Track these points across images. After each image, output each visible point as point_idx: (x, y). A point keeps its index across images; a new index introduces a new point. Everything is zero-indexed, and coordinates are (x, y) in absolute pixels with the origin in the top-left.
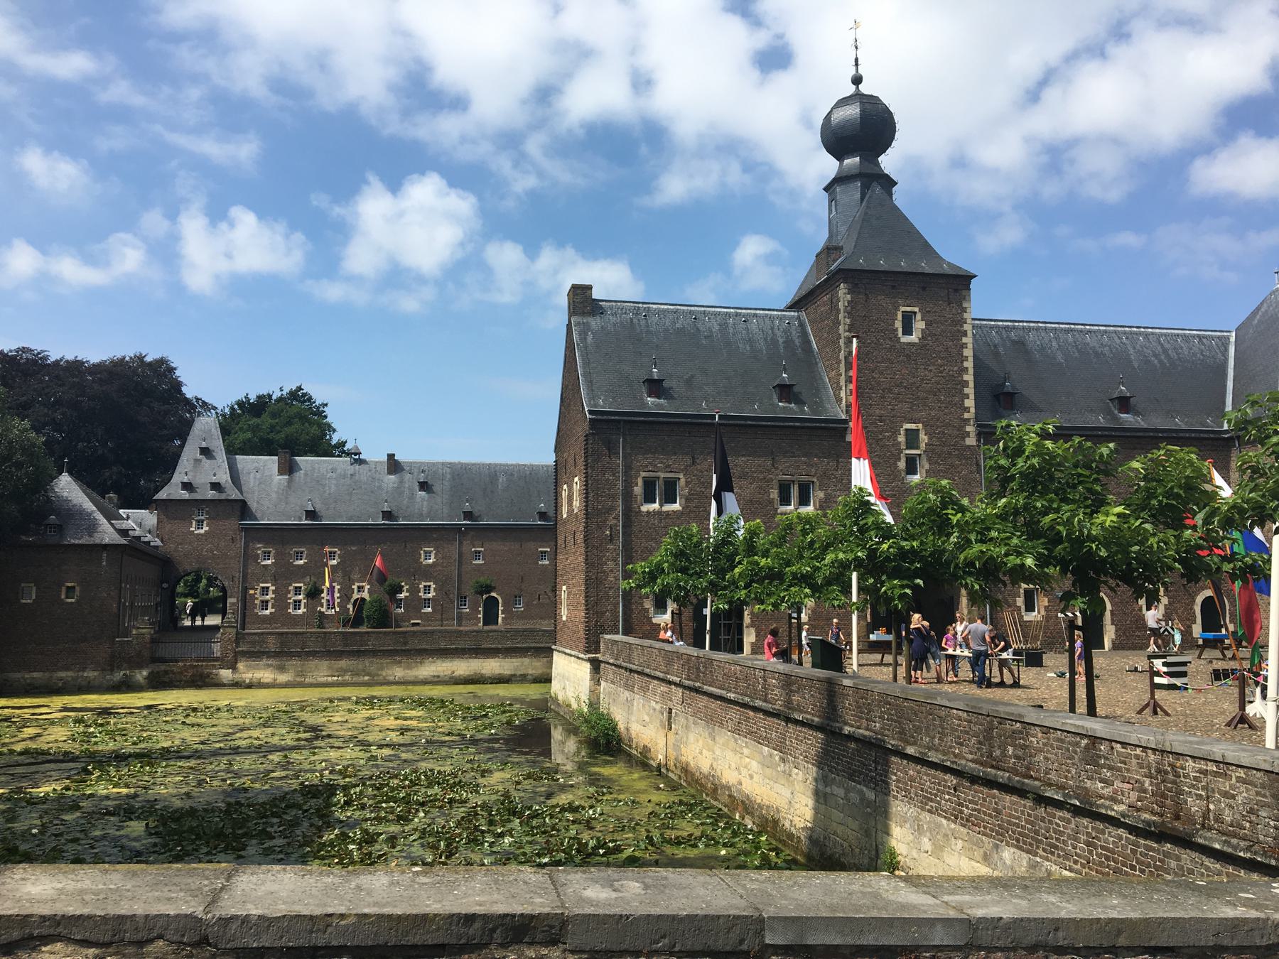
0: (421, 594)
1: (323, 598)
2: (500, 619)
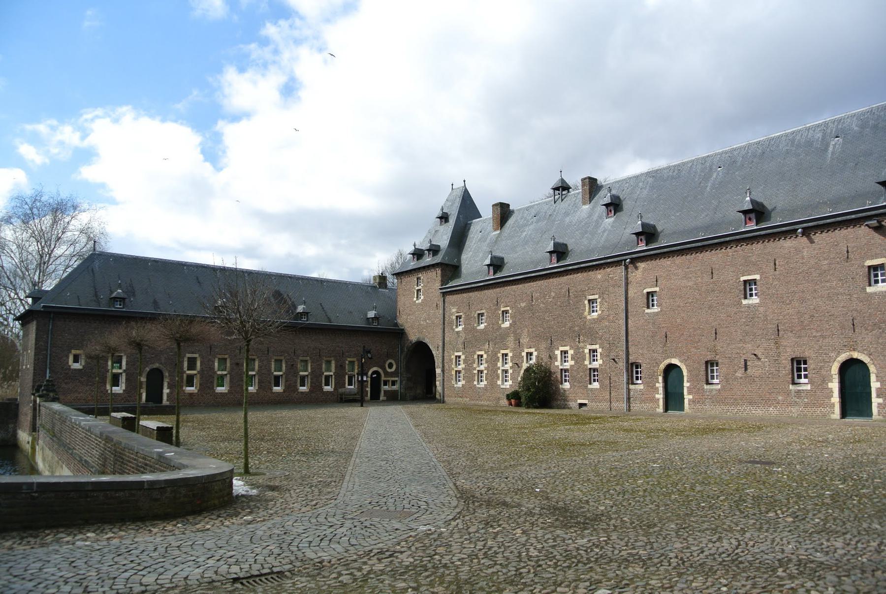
0: (587, 362)
1: (499, 368)
2: (686, 402)
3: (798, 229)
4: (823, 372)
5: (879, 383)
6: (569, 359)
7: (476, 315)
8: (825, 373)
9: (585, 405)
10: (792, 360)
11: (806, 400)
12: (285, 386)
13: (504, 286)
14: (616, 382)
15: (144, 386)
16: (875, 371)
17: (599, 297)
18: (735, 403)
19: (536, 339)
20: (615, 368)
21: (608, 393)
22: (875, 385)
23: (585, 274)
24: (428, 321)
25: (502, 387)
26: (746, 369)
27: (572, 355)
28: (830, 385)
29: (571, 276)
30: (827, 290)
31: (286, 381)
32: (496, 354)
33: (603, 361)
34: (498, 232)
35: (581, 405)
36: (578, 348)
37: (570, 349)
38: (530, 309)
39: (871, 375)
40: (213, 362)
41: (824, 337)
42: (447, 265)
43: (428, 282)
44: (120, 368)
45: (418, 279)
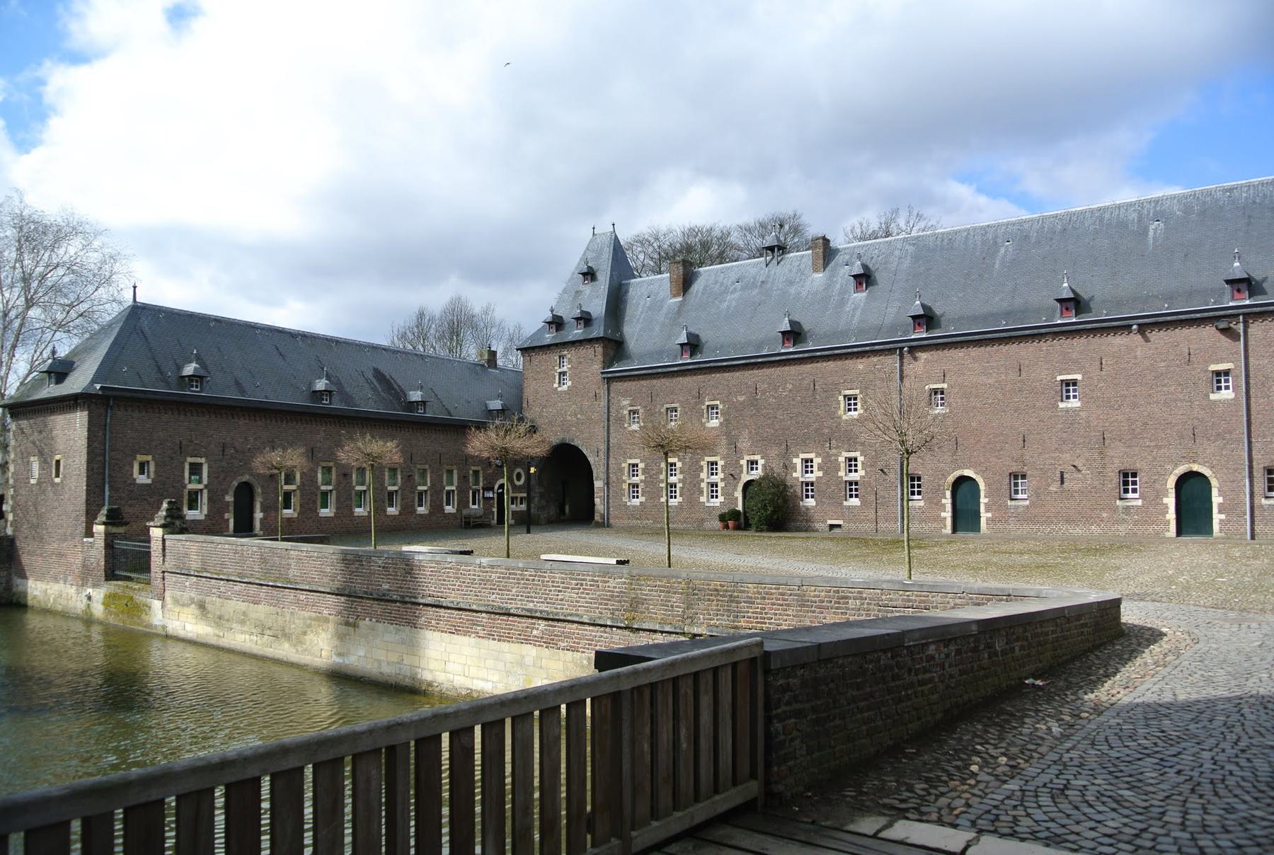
0: (842, 473)
1: (703, 480)
2: (983, 521)
3: (1132, 325)
4: (1157, 486)
5: (1221, 498)
6: (815, 469)
7: (663, 410)
8: (1159, 487)
9: (839, 526)
10: (1119, 472)
11: (1136, 517)
12: (401, 505)
13: (710, 373)
14: (884, 498)
15: (231, 508)
16: (1218, 485)
17: (861, 393)
18: (1049, 521)
19: (761, 444)
20: (884, 481)
21: (873, 512)
22: (1216, 499)
23: (839, 363)
24: (579, 416)
25: (707, 504)
26: (1062, 482)
27: (819, 464)
28: (1165, 500)
29: (819, 365)
30: (1165, 395)
31: (402, 499)
32: (697, 462)
33: (866, 471)
34: (680, 299)
35: (832, 527)
36: (829, 455)
37: (816, 457)
38: (752, 405)
39: (1213, 489)
40: (316, 473)
41: (1158, 447)
42: (610, 340)
44: (200, 482)
45: (560, 357)
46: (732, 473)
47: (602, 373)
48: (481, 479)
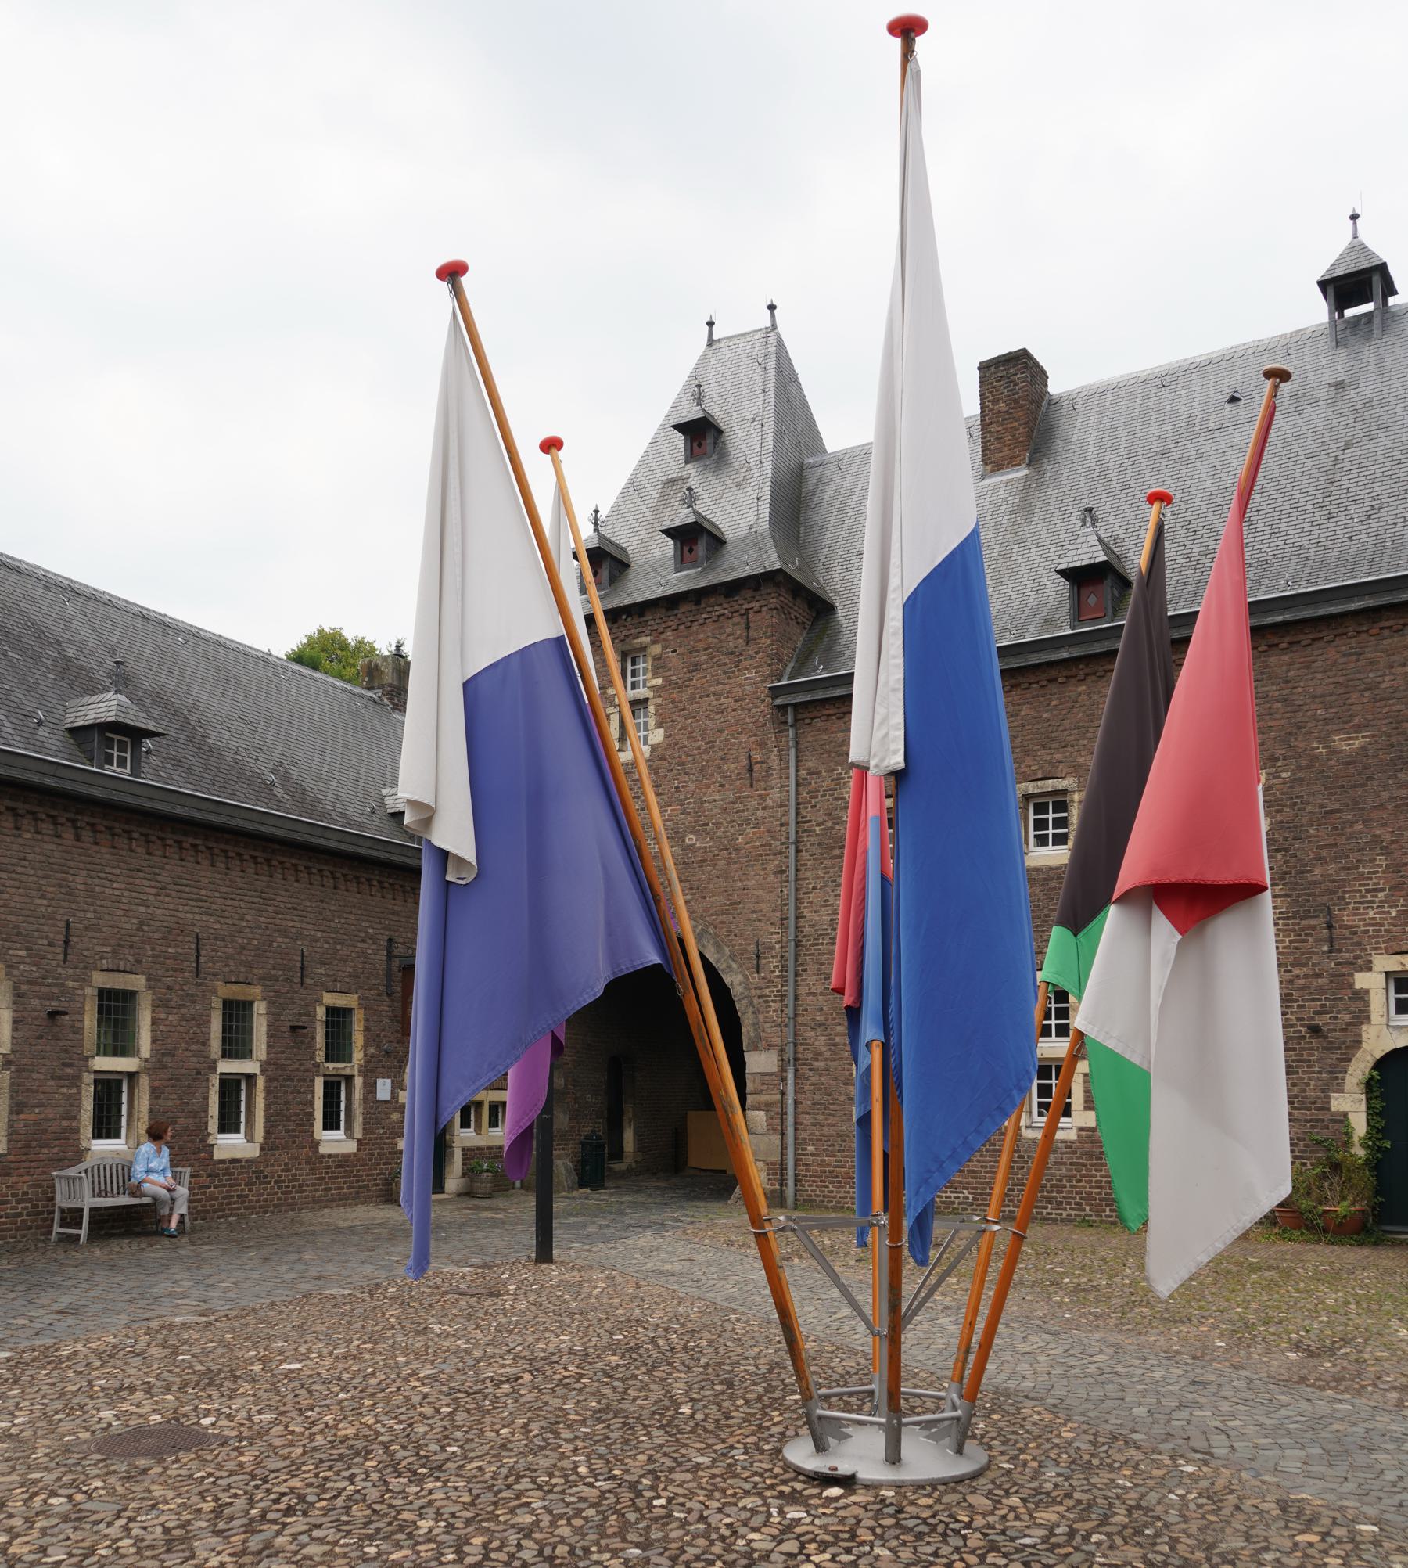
24: (690, 839)
43: (696, 668)
46: (1319, 1020)
47: (775, 692)
48: (358, 1039)
